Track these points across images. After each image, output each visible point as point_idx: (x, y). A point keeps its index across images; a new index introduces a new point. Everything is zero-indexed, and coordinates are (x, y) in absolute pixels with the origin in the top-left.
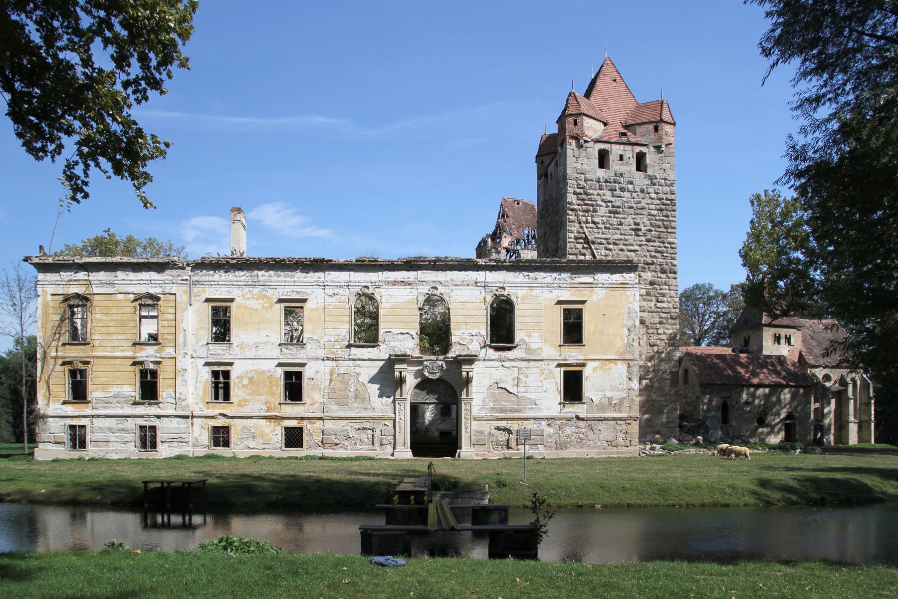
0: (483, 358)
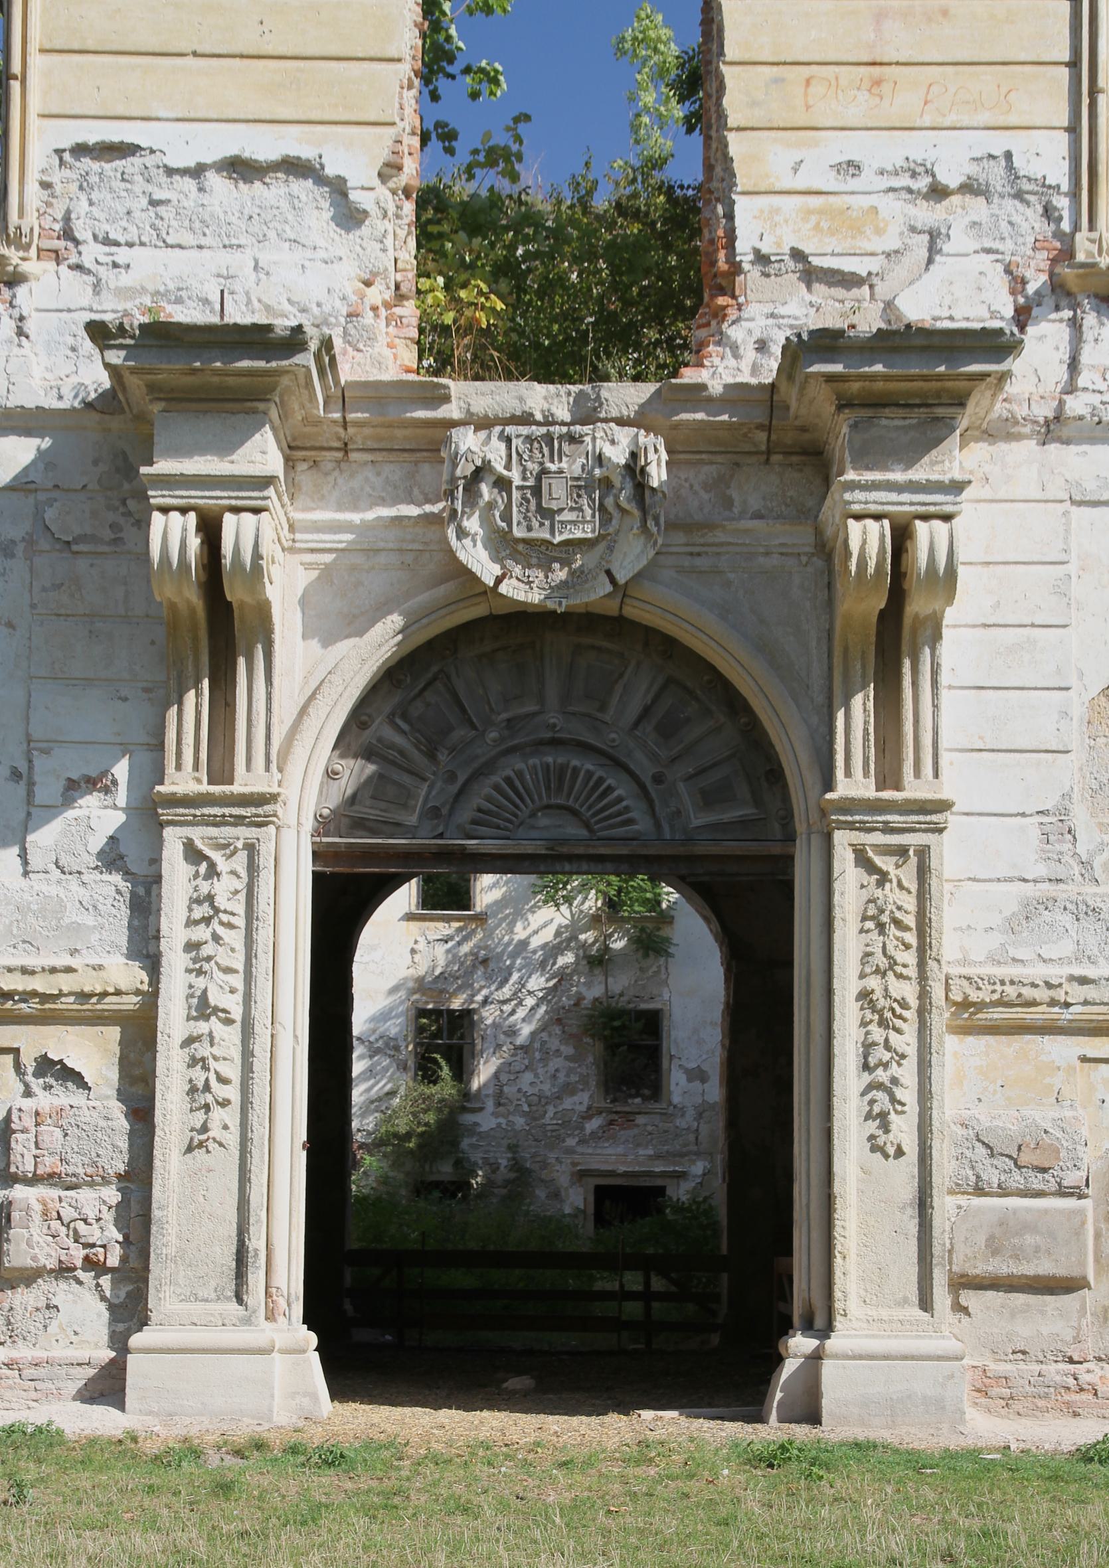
0: (1044, 411)
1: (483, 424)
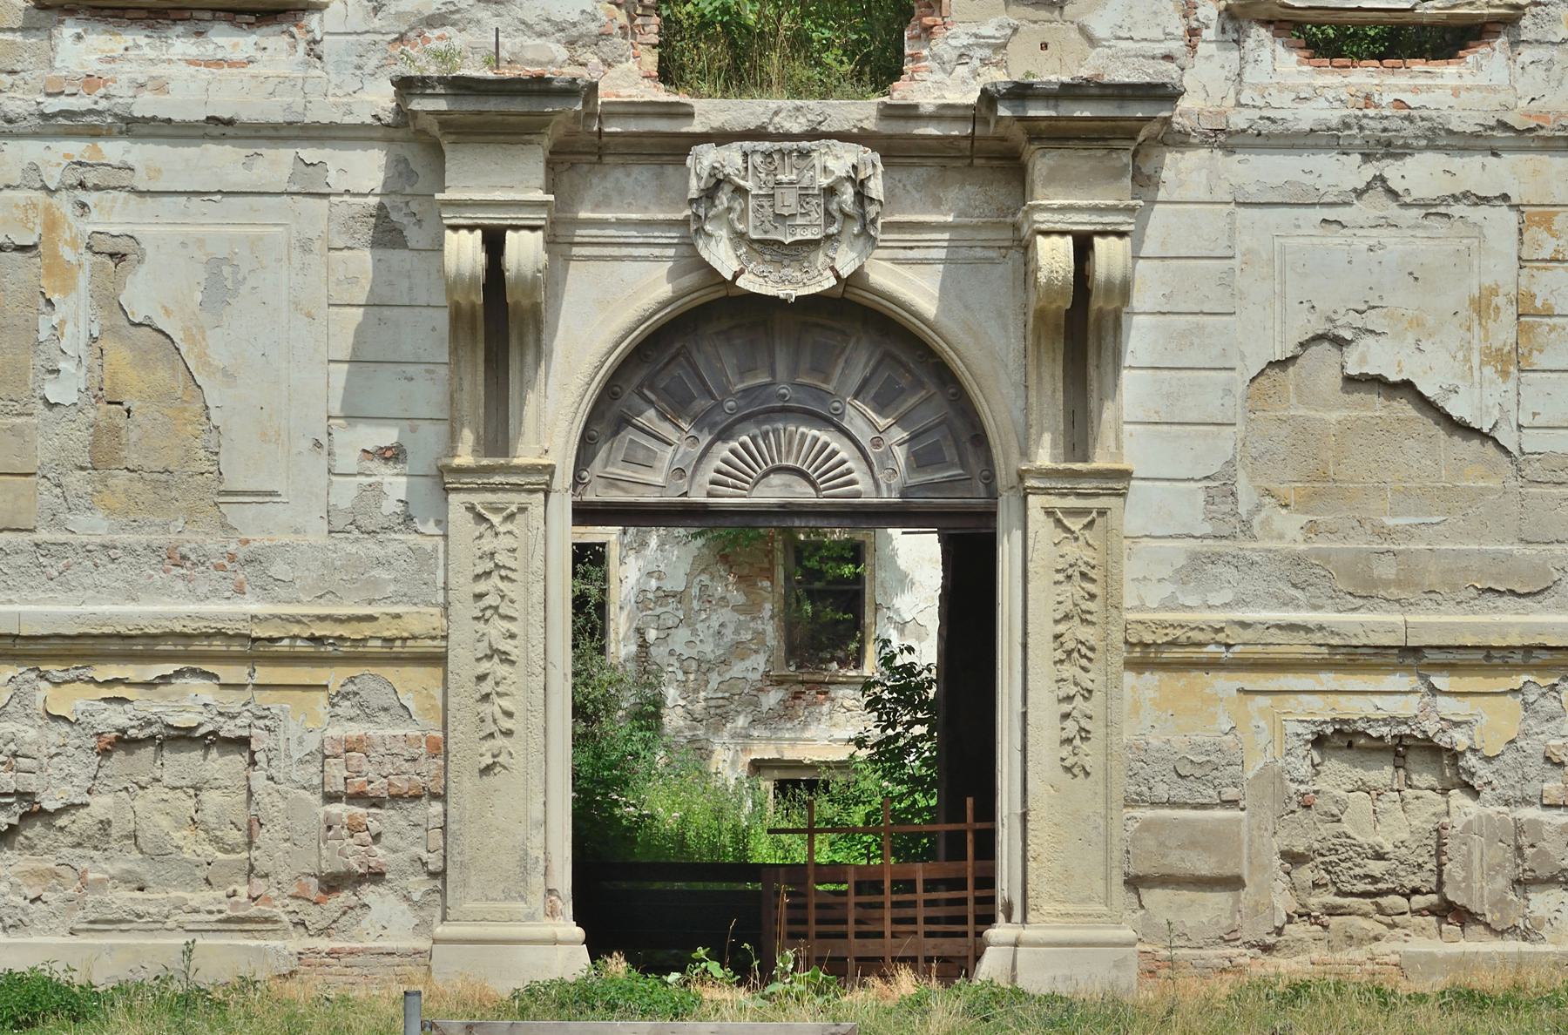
1: (721, 137)
